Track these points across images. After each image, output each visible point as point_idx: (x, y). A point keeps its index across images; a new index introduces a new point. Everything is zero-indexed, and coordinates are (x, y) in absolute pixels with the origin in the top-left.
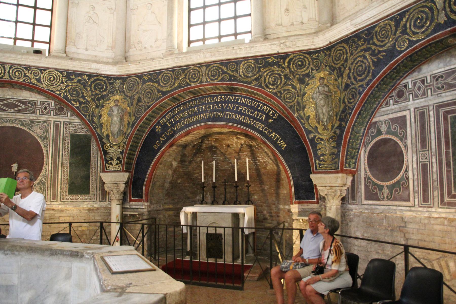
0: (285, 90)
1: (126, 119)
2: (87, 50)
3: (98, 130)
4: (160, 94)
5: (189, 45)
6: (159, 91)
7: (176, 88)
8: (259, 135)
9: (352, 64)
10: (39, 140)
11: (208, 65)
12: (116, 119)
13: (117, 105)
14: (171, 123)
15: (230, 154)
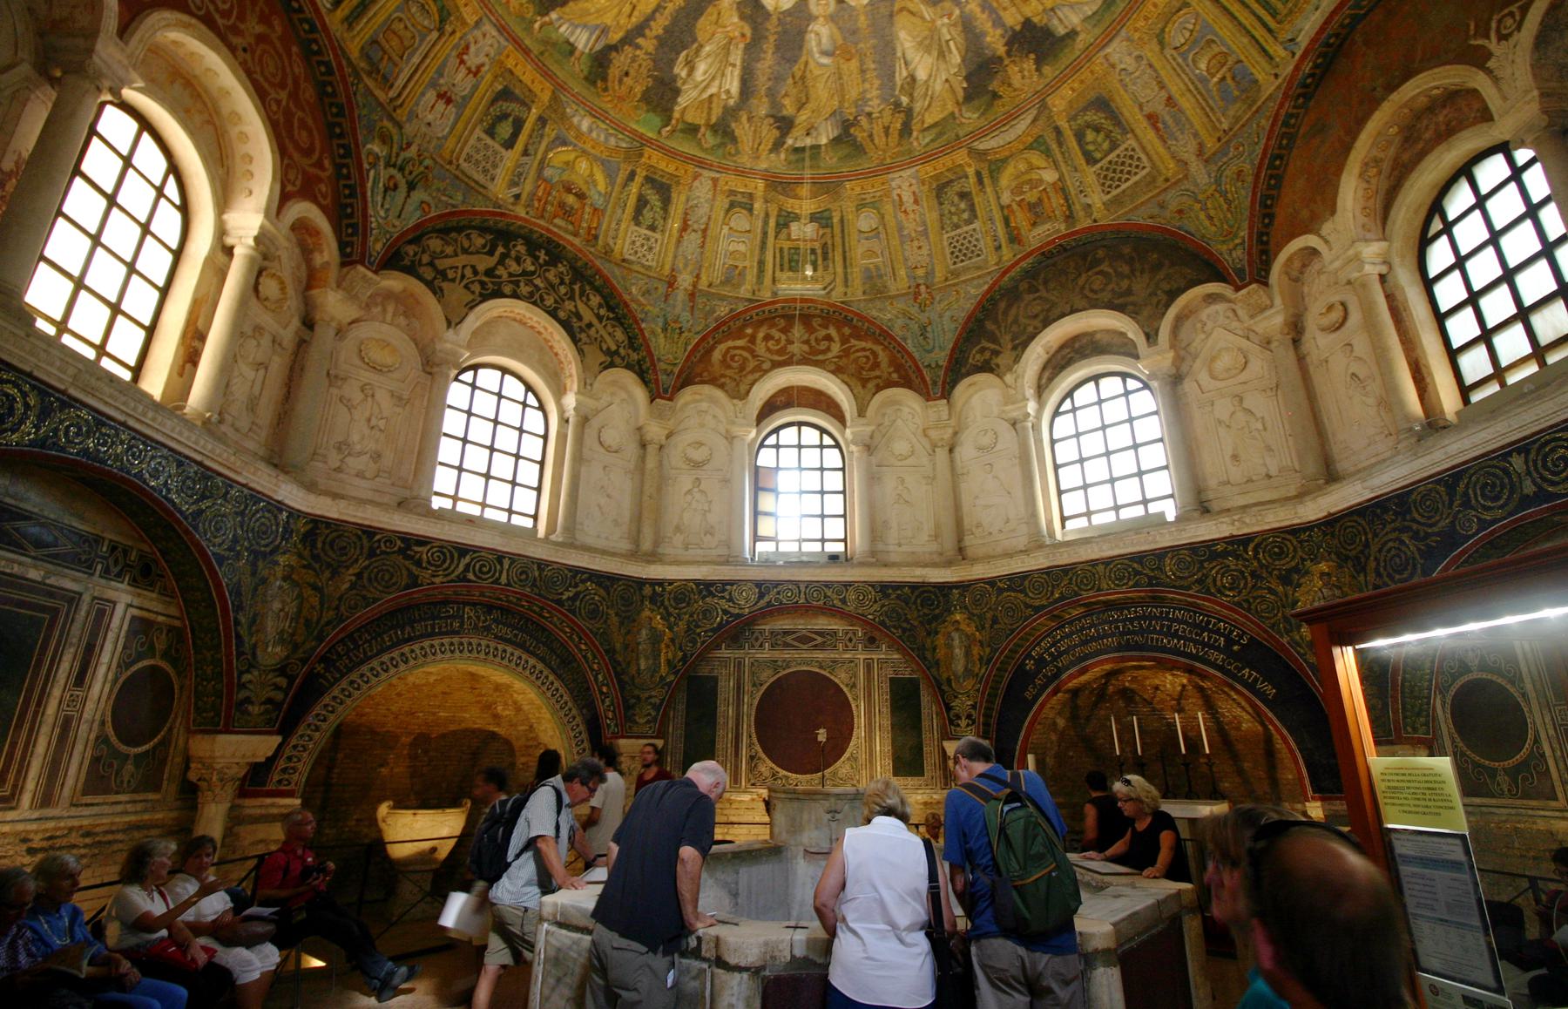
0: (1255, 598)
1: (976, 650)
2: (900, 545)
3: (934, 670)
4: (1029, 611)
5: (1063, 527)
6: (1027, 606)
7: (1056, 601)
8: (1219, 674)
9: (1380, 551)
10: (845, 689)
11: (1107, 562)
12: (958, 652)
13: (957, 630)
14: (1051, 654)
15: (1162, 701)
